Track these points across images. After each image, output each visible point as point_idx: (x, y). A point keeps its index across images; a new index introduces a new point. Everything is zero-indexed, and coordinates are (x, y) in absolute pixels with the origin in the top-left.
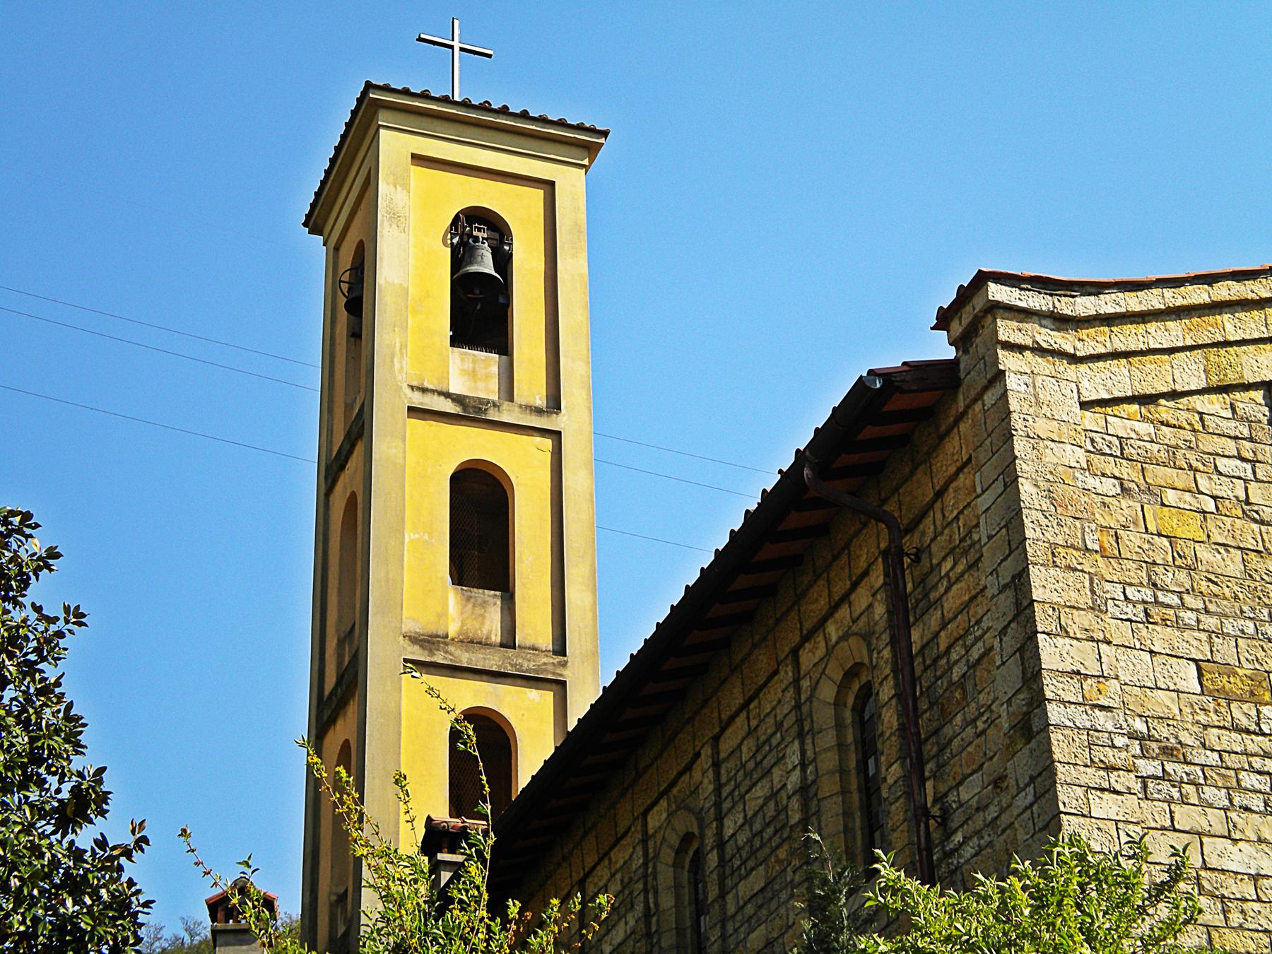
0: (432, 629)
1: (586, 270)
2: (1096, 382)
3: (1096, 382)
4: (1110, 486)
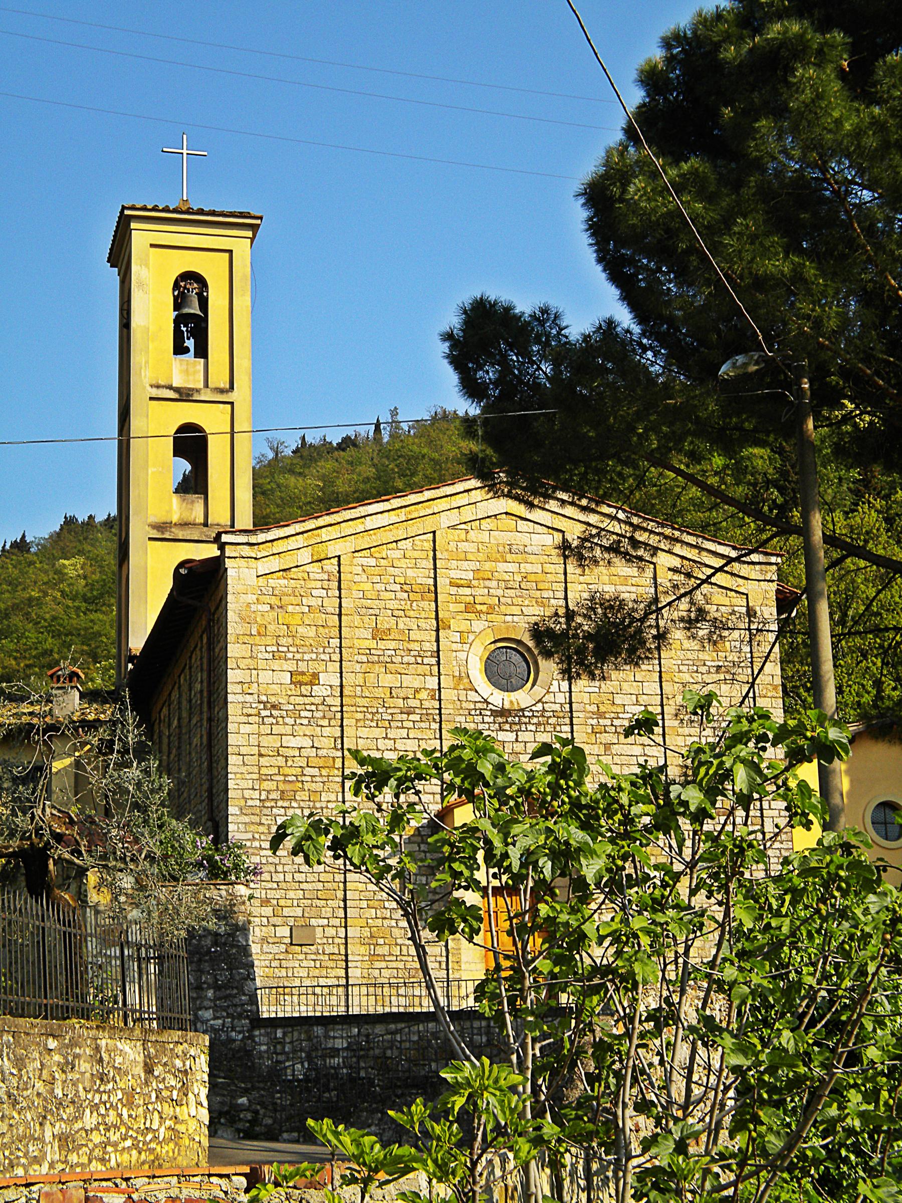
0: (164, 519)
1: (249, 304)
2: (263, 567)
3: (263, 567)
4: (267, 607)
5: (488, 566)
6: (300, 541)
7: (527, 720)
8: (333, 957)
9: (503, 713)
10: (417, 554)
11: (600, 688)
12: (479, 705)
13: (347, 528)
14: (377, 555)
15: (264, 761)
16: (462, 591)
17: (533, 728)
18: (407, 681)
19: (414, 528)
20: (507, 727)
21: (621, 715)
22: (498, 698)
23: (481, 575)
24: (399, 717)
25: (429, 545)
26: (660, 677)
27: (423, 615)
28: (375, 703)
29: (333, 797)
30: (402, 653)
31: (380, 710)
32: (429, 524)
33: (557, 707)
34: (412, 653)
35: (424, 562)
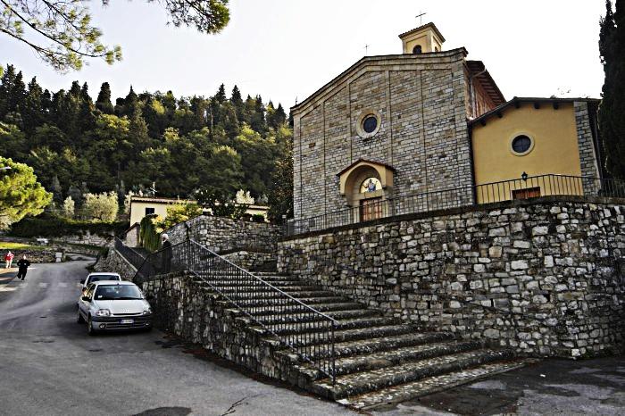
2: (302, 115)
9: (366, 140)
18: (338, 138)
22: (366, 135)
32: (344, 85)
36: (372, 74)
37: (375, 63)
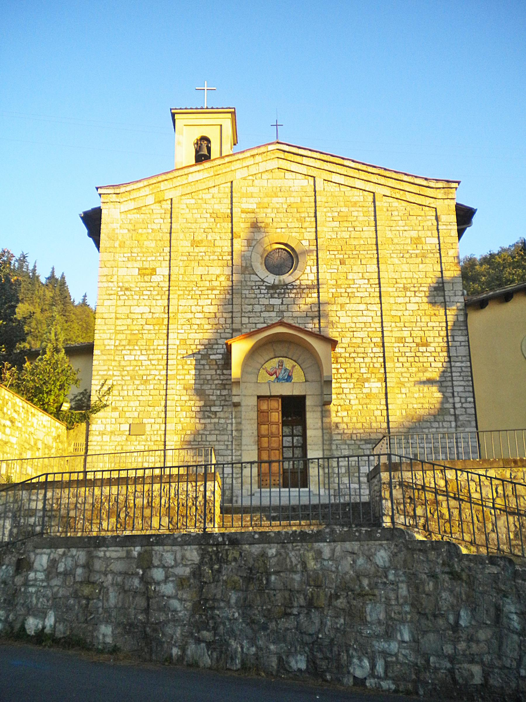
2: (124, 207)
3: (124, 207)
5: (266, 200)
6: (147, 190)
7: (289, 291)
8: (157, 443)
9: (274, 287)
10: (220, 195)
11: (338, 269)
12: (258, 283)
13: (177, 182)
14: (196, 197)
15: (119, 322)
16: (249, 215)
17: (293, 296)
18: (212, 270)
19: (219, 180)
20: (276, 296)
21: (352, 286)
22: (271, 279)
23: (261, 206)
24: (206, 292)
25: (228, 190)
26: (378, 261)
27: (224, 231)
28: (191, 285)
29: (161, 342)
30: (209, 254)
31: (194, 289)
33: (310, 283)
34: (216, 254)
35: (226, 200)
36: (288, 175)
37: (298, 159)
